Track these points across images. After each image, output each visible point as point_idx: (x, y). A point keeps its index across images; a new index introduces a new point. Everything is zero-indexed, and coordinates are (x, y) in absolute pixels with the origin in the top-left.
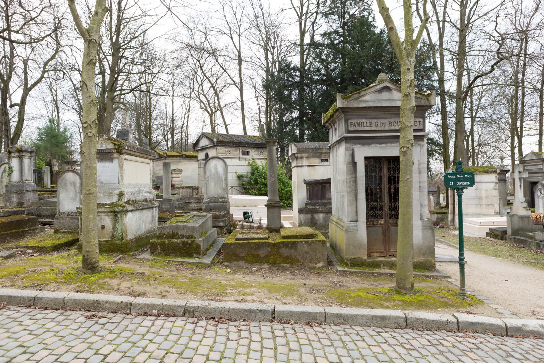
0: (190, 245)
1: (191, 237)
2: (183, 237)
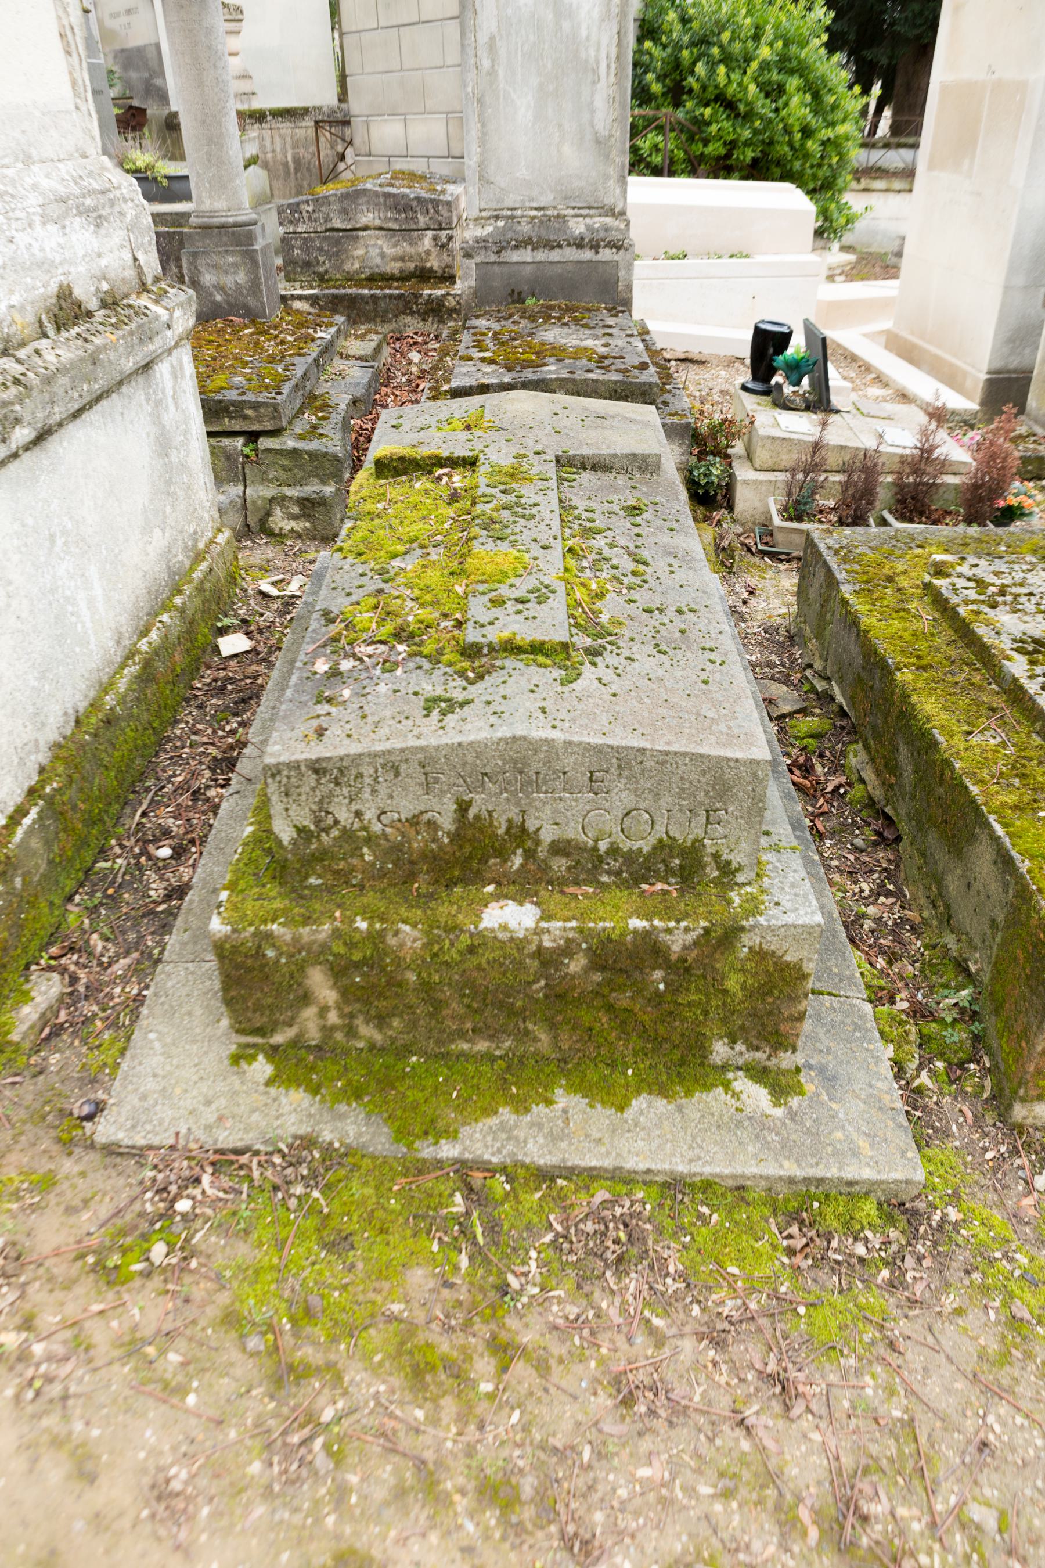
0: (681, 970)
1: (684, 866)
2: (588, 864)
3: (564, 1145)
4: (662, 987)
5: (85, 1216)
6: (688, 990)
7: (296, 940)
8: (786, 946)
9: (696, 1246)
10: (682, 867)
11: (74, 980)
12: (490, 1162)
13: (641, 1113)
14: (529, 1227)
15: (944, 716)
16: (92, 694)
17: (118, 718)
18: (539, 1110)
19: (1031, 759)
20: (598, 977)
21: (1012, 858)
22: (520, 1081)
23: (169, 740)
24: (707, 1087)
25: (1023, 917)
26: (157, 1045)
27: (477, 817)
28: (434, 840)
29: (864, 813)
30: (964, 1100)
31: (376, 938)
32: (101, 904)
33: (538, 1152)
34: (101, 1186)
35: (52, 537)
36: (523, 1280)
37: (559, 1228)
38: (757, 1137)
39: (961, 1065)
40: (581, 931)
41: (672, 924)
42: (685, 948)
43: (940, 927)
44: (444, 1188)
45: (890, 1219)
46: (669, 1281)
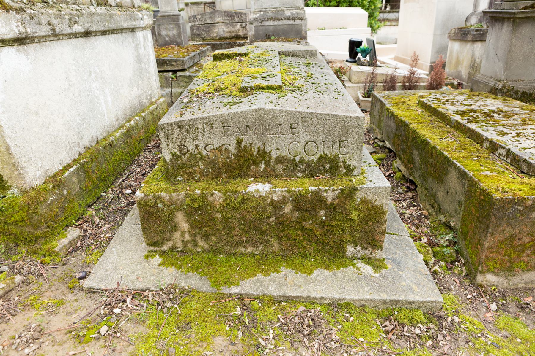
0: (332, 208)
1: (330, 166)
2: (291, 167)
3: (285, 288)
4: (324, 218)
5: (74, 316)
6: (335, 220)
7: (171, 199)
8: (375, 197)
9: (344, 329)
10: (330, 168)
11: (85, 231)
12: (253, 295)
13: (318, 275)
14: (269, 321)
15: (430, 134)
16: (105, 135)
17: (115, 146)
18: (274, 275)
19: (467, 144)
20: (297, 214)
21: (465, 172)
22: (266, 263)
23: (136, 160)
24: (346, 266)
25: (473, 194)
26: (115, 252)
27: (245, 146)
28: (228, 158)
29: (401, 182)
30: (455, 276)
31: (204, 196)
32: (101, 208)
33: (274, 291)
34: (83, 305)
35: (90, 73)
36: (267, 342)
37: (283, 321)
38: (368, 284)
39: (452, 263)
40: (289, 192)
41: (327, 188)
42: (333, 199)
43: (436, 215)
44: (232, 304)
45: (429, 319)
46: (333, 343)
